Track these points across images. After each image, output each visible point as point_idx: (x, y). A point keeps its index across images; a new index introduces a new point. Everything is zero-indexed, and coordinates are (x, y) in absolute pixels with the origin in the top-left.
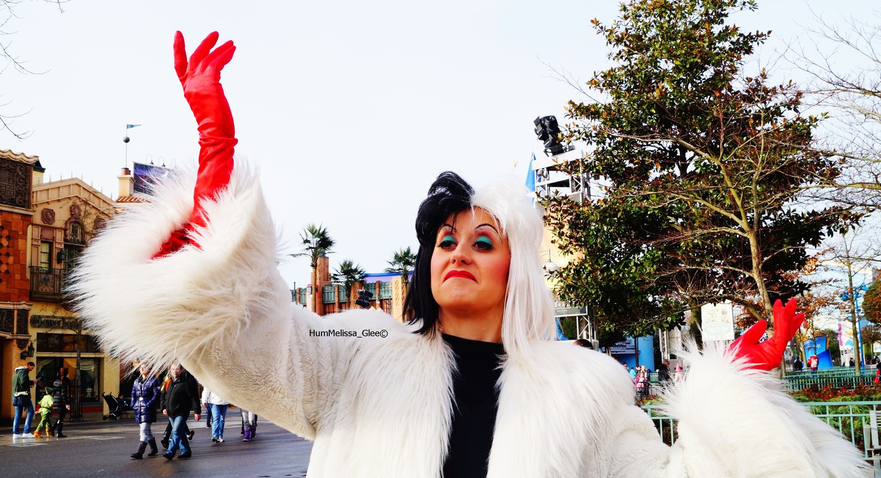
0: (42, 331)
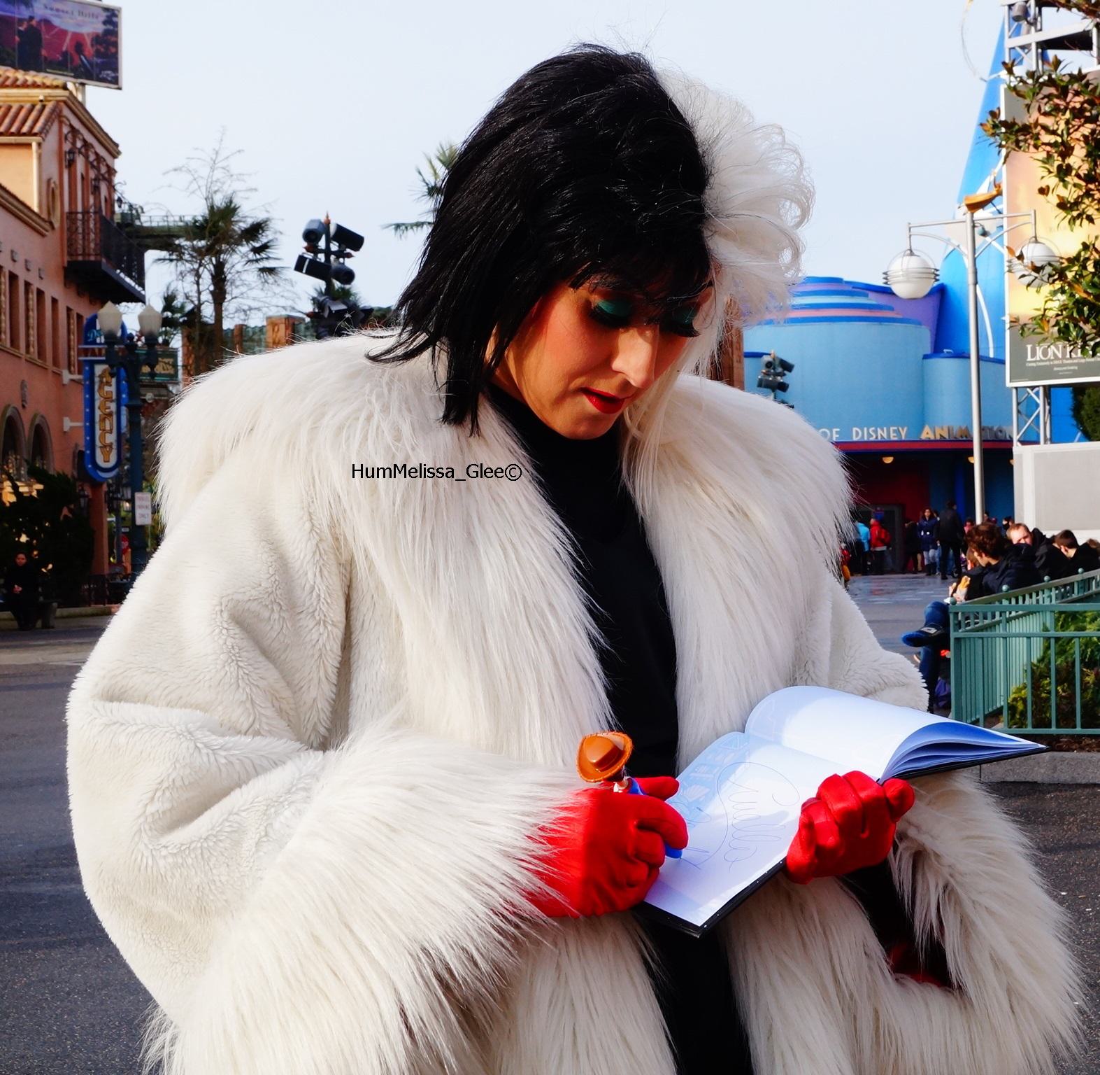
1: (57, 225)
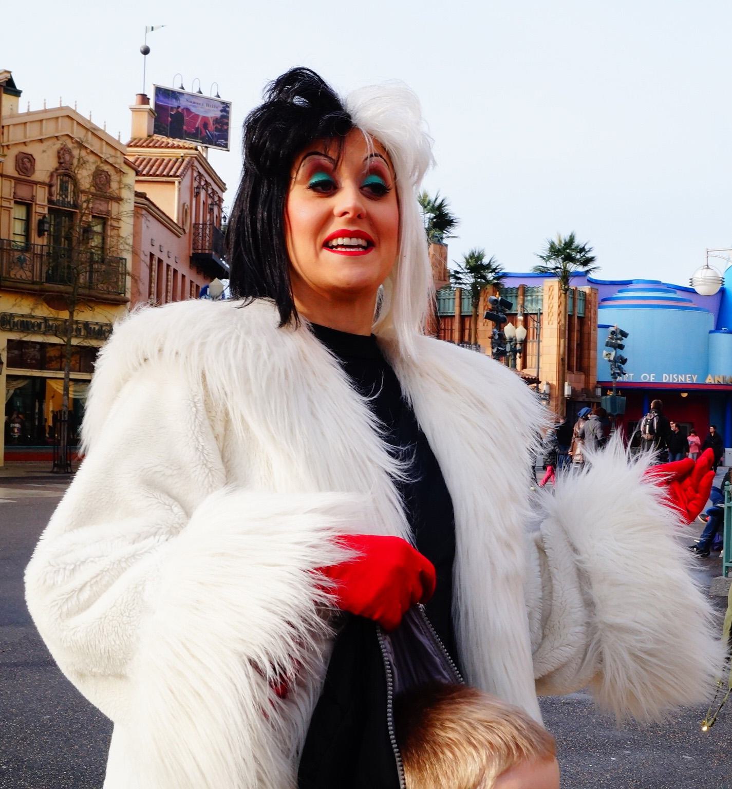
0: (14, 336)
1: (187, 231)
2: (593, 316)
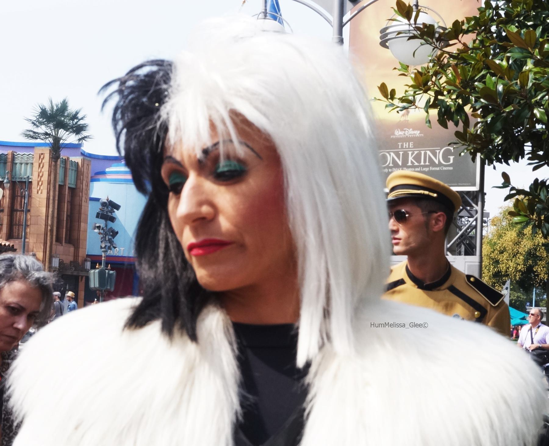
2: (84, 187)
